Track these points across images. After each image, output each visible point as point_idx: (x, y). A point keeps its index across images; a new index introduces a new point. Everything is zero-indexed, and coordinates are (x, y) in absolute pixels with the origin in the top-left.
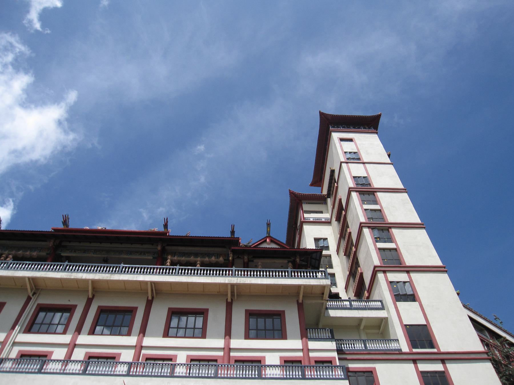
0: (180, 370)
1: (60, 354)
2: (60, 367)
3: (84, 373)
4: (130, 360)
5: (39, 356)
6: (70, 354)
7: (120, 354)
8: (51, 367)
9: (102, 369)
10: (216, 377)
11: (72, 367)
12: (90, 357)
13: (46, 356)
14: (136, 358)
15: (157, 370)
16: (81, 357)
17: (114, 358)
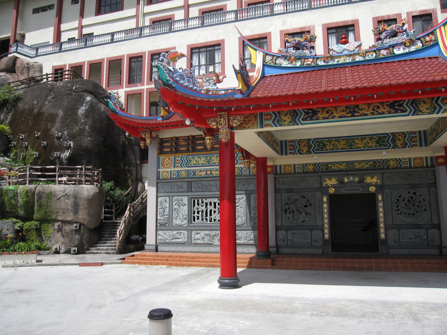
0: (278, 9)
1: (179, 15)
2: (183, 25)
3: (203, 25)
4: (235, 8)
5: (166, 20)
6: (187, 13)
7: (226, 6)
8: (177, 26)
9: (215, 20)
10: (310, 8)
11: (192, 23)
12: (203, 13)
13: (170, 19)
14: (239, 6)
15: (259, 13)
16: (197, 14)
17: (222, 9)
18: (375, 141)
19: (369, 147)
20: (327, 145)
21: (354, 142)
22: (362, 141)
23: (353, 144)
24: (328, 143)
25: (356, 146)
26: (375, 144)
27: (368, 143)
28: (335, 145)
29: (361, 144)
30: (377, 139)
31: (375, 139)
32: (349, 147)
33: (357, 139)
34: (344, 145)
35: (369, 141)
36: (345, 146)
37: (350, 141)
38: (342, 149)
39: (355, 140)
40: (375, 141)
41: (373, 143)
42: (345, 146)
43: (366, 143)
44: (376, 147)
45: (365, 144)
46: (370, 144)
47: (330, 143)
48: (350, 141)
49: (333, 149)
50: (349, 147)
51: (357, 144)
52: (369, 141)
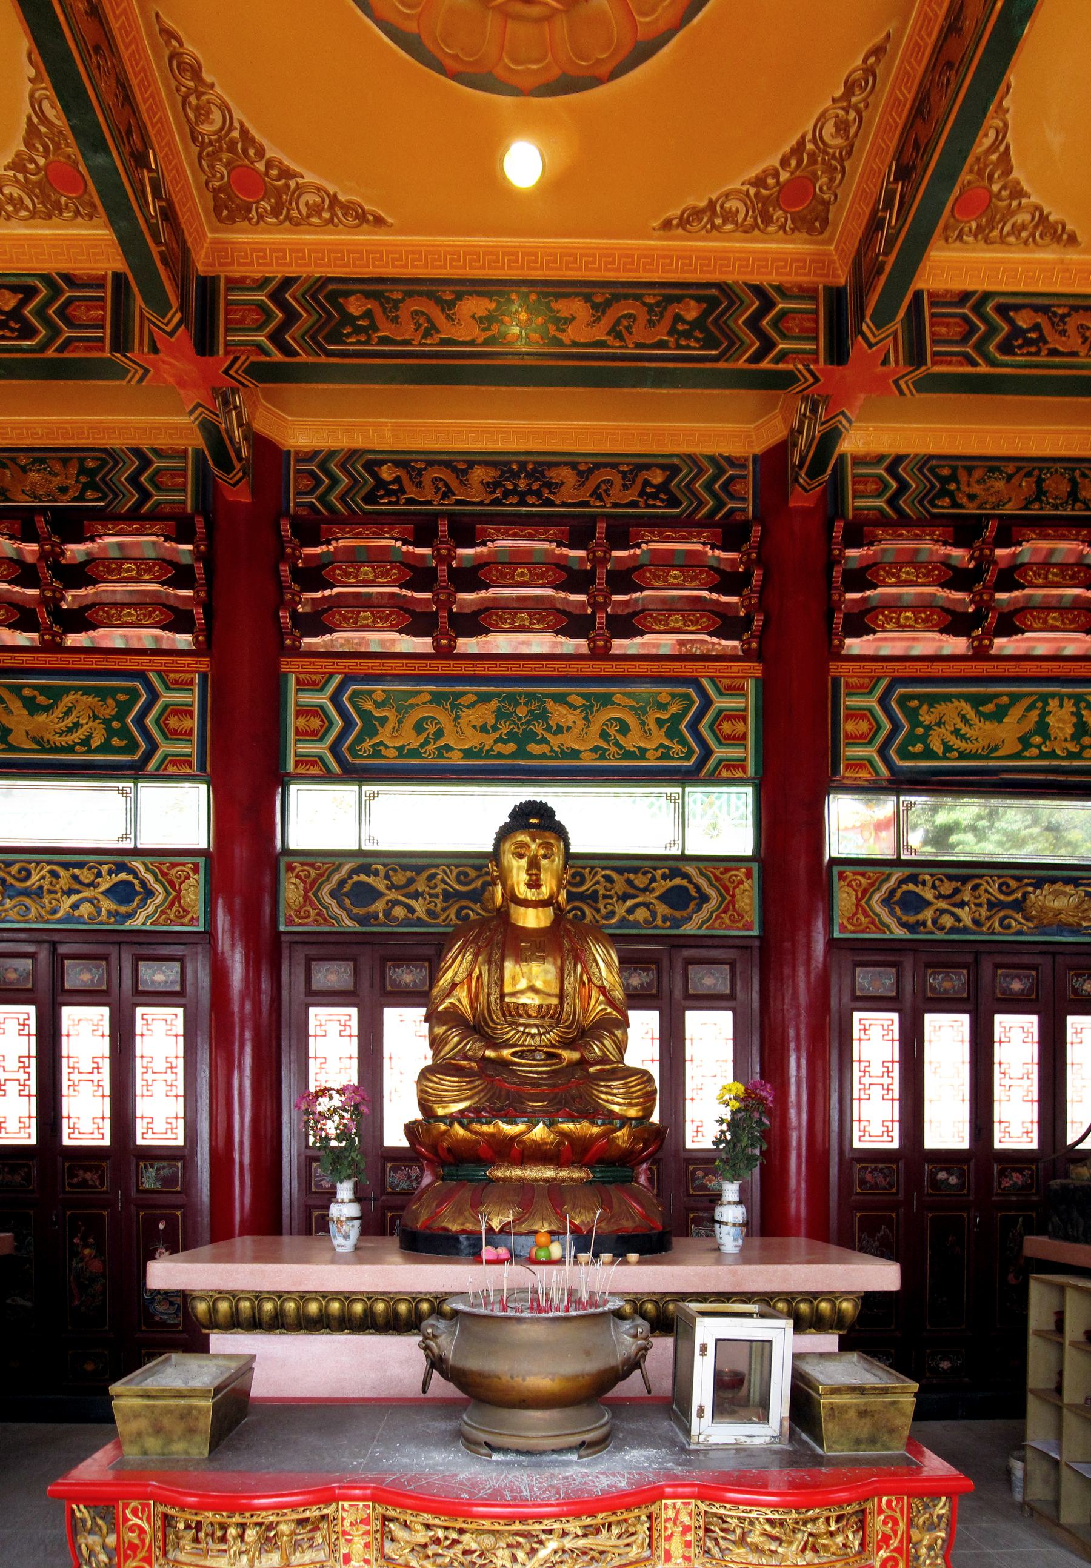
18: (660, 722)
19: (628, 755)
20: (383, 720)
21: (543, 716)
22: (588, 711)
23: (539, 729)
24: (390, 713)
25: (555, 741)
26: (659, 737)
27: (624, 729)
28: (432, 730)
29: (583, 735)
30: (674, 709)
31: (663, 707)
32: (511, 747)
33: (560, 699)
34: (484, 729)
35: (630, 720)
36: (488, 740)
37: (522, 711)
38: (468, 753)
39: (550, 704)
40: (660, 722)
41: (647, 734)
42: (488, 740)
43: (612, 731)
44: (664, 756)
45: (604, 735)
46: (631, 742)
47: (403, 711)
48: (522, 711)
49: (415, 753)
50: (511, 747)
51: (559, 730)
52: (630, 720)
